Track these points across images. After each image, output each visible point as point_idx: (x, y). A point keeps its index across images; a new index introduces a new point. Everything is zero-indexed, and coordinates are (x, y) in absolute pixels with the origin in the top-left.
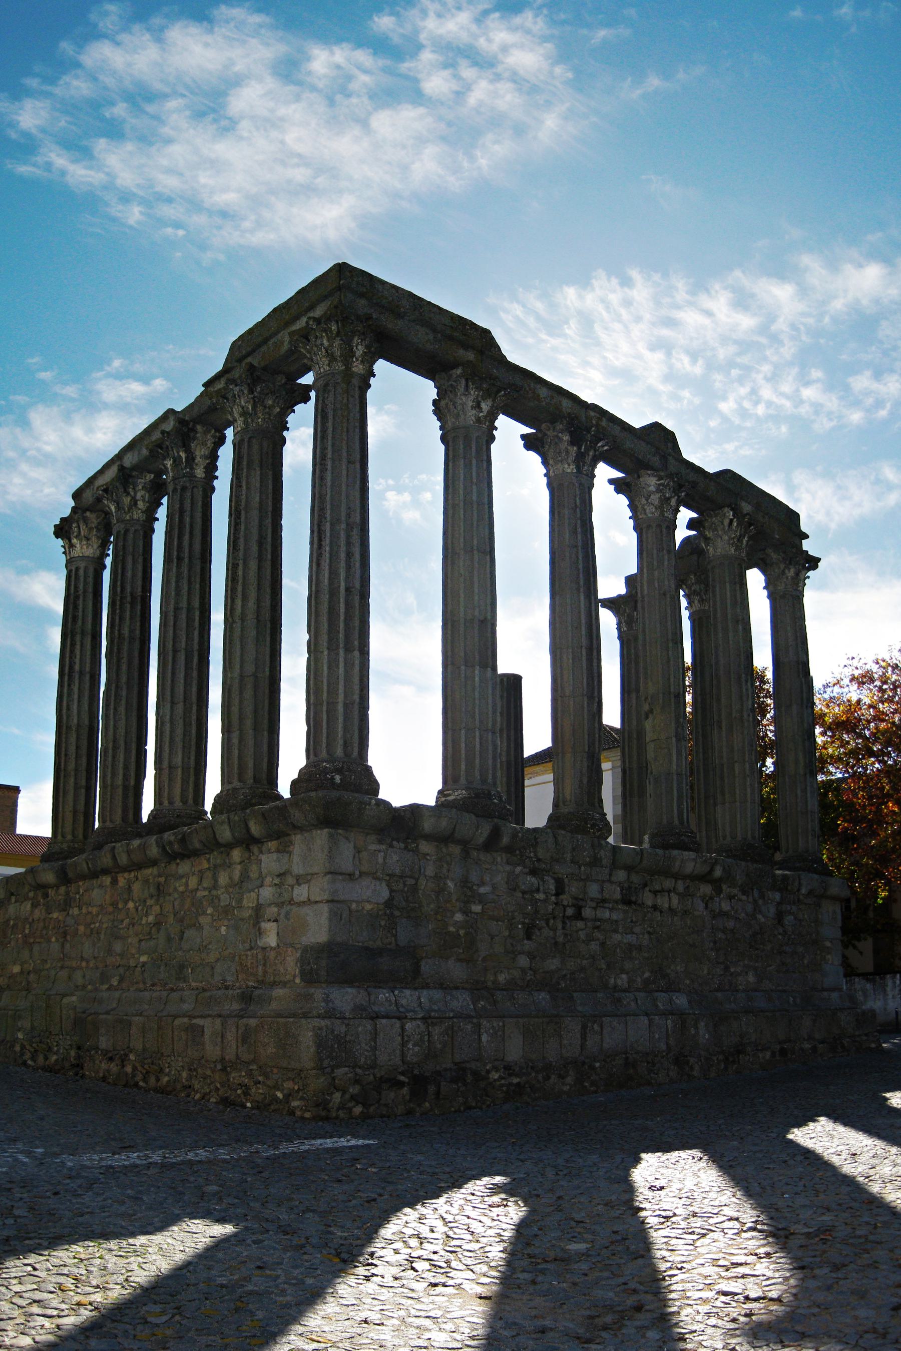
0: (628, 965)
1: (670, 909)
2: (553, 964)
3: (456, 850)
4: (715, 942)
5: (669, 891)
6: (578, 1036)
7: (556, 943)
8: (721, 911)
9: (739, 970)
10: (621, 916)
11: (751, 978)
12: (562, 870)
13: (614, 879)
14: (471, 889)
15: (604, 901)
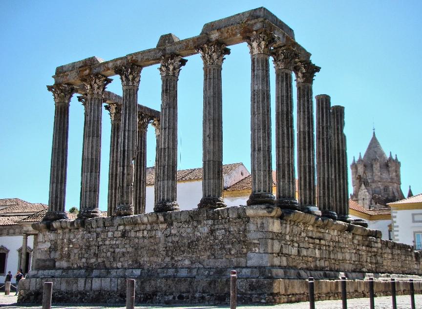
0: (122, 259)
1: (143, 237)
2: (93, 261)
3: (67, 230)
4: (166, 248)
5: (143, 230)
6: (84, 283)
7: (95, 254)
8: (171, 233)
9: (180, 258)
10: (120, 242)
11: (187, 262)
12: (99, 230)
13: (119, 229)
14: (70, 240)
15: (115, 237)
